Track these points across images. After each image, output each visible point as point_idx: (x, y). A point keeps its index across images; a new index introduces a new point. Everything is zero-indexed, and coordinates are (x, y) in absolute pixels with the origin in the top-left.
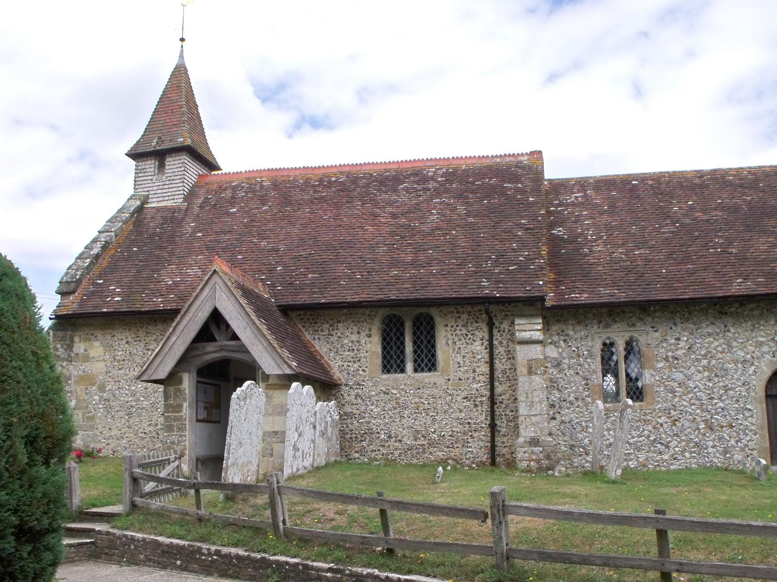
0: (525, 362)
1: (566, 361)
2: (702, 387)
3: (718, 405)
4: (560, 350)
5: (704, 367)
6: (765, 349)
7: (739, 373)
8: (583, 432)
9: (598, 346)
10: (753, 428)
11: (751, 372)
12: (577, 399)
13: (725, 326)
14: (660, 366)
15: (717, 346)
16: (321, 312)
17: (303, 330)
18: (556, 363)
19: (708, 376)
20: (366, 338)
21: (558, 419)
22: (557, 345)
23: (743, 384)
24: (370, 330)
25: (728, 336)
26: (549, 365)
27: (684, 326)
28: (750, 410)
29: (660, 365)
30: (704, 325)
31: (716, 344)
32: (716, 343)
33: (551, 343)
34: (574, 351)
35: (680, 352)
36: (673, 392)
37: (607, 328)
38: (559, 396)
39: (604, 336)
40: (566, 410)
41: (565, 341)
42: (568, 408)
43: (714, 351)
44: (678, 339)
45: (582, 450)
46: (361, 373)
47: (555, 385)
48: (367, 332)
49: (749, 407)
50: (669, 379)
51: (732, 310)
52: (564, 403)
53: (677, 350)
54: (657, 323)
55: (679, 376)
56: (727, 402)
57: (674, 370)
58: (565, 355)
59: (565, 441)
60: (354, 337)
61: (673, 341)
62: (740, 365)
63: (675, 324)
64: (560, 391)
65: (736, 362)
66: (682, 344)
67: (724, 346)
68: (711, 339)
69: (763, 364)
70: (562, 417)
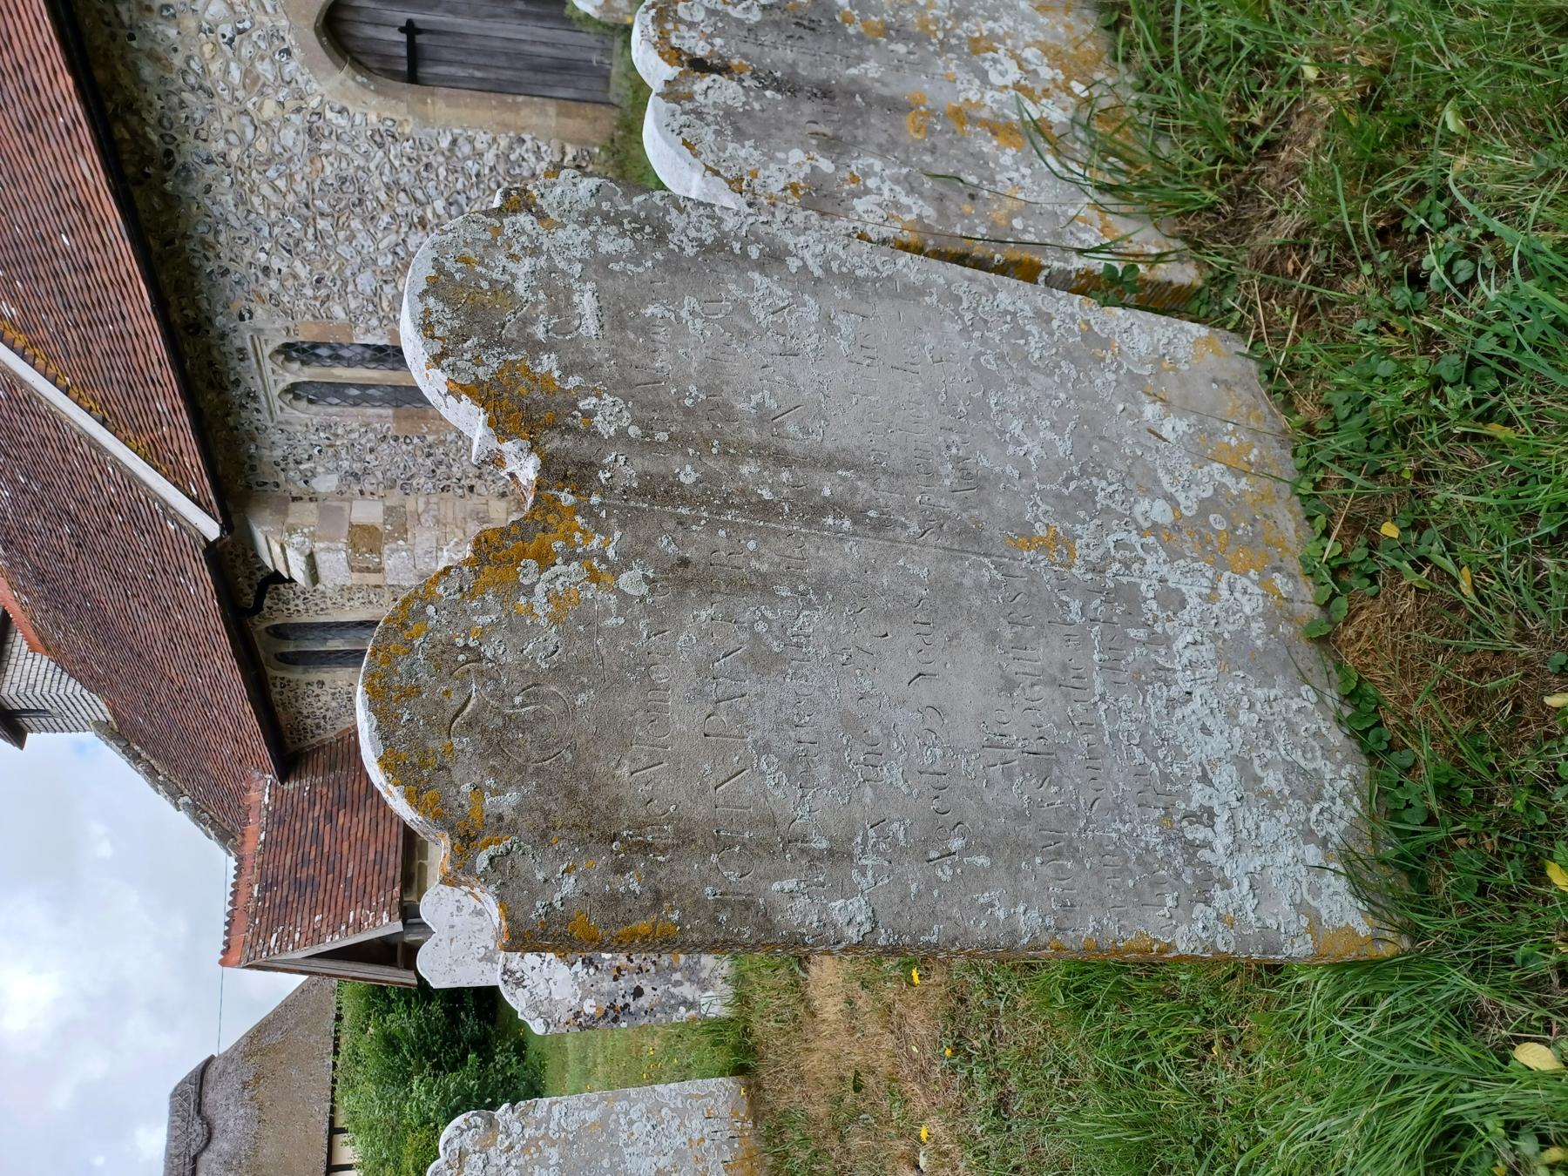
0: (355, 575)
1: (345, 464)
2: (393, 238)
3: (441, 211)
4: (320, 469)
5: (335, 226)
6: (265, 69)
7: (348, 150)
9: (302, 415)
10: (503, 143)
11: (342, 121)
12: (429, 455)
13: (209, 161)
14: (342, 315)
15: (275, 189)
16: (283, 719)
17: (318, 738)
18: (351, 478)
19: (363, 222)
20: (326, 687)
21: (473, 483)
22: (309, 474)
23: (381, 146)
25: (240, 159)
26: (356, 488)
27: (225, 253)
28: (454, 142)
29: (338, 311)
30: (216, 210)
31: (267, 189)
32: (266, 190)
33: (306, 482)
34: (320, 451)
35: (302, 271)
37: (255, 398)
38: (422, 481)
39: (278, 403)
40: (454, 469)
41: (298, 463)
42: (450, 466)
43: (291, 198)
44: (266, 270)
47: (400, 482)
48: (315, 687)
49: (445, 143)
50: (376, 300)
51: (155, 138)
52: (438, 472)
53: (295, 277)
54: (226, 306)
55: (366, 281)
56: (433, 192)
57: (351, 288)
58: (331, 465)
60: (323, 699)
61: (274, 284)
62: (325, 146)
63: (225, 272)
64: (412, 476)
65: (315, 154)
66: (276, 263)
67: (271, 173)
68: (256, 201)
69: (315, 86)
70: (467, 477)
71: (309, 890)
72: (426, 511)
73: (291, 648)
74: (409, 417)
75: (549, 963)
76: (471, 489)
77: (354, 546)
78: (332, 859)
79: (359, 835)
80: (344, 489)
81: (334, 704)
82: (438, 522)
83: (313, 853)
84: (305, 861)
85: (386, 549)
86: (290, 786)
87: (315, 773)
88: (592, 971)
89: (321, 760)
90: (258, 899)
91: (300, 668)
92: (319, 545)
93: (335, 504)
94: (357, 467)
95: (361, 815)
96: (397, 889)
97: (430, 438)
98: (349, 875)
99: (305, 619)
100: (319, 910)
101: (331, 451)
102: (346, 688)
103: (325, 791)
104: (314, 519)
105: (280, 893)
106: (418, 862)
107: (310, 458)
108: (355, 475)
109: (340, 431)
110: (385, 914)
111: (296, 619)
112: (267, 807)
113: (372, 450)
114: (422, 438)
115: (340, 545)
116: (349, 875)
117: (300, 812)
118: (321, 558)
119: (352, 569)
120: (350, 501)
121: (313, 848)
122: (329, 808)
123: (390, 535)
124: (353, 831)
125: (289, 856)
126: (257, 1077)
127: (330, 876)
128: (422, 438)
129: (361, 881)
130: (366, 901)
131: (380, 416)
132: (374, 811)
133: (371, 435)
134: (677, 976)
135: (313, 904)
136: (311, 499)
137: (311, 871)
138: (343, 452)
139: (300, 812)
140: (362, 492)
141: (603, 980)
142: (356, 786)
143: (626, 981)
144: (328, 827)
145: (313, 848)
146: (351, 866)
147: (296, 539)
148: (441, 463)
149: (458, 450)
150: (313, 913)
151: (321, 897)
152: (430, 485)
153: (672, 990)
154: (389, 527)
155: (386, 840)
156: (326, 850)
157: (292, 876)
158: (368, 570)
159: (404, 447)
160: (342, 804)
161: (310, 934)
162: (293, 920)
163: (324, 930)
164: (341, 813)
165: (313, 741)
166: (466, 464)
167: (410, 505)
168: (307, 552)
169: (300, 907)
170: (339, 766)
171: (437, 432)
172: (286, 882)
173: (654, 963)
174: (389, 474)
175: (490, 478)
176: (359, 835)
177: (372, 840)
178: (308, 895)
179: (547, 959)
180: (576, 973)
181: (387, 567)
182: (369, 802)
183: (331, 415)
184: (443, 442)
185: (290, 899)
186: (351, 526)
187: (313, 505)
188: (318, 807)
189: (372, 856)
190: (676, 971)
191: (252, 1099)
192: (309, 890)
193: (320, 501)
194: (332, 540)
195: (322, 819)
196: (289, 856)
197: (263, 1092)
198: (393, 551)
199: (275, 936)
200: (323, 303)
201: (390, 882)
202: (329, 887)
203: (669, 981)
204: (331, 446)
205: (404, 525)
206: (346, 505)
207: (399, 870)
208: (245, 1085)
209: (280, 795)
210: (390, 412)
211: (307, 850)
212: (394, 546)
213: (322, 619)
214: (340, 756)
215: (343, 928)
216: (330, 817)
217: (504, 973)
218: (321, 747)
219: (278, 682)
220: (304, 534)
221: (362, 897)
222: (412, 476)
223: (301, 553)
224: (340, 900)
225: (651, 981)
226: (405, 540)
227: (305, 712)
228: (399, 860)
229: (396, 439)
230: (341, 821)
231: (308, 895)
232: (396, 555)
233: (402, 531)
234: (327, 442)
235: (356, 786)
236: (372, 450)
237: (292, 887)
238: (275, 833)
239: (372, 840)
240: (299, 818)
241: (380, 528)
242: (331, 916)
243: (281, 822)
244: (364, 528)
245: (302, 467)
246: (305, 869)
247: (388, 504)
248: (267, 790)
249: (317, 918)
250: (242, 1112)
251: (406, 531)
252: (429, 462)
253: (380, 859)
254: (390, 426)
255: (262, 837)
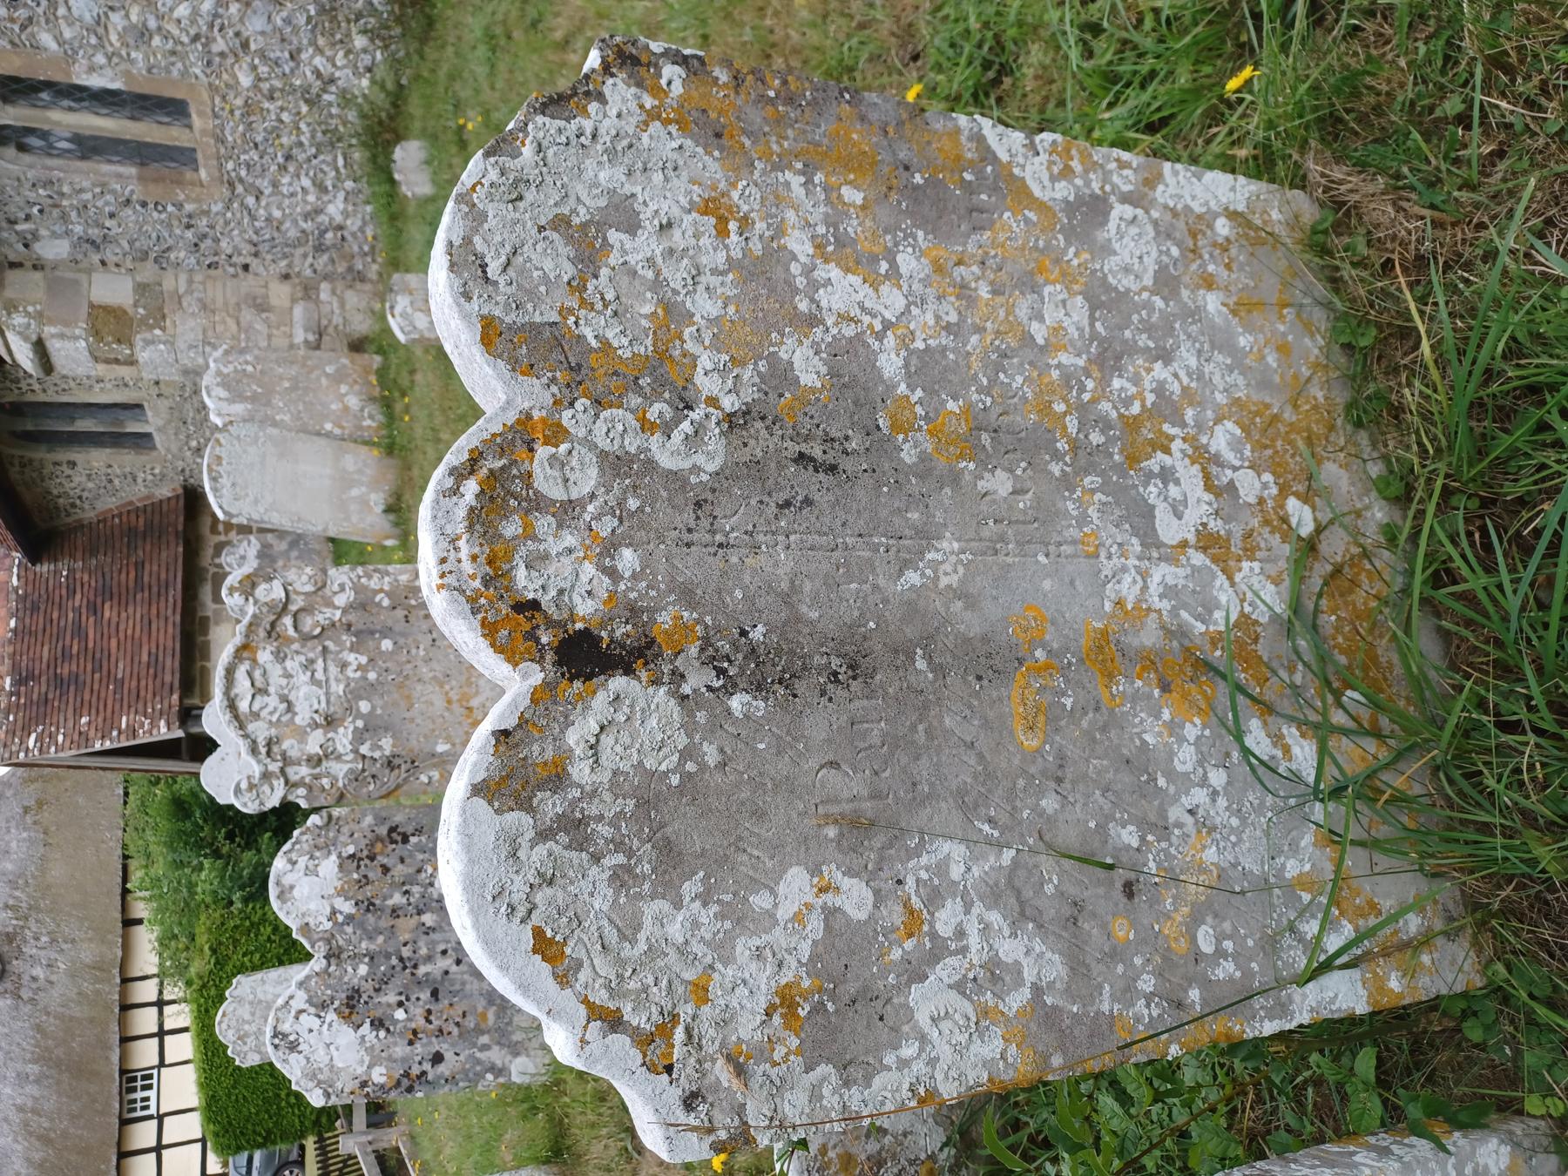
1: (78, 229)
4: (43, 232)
8: (283, 228)
12: (189, 226)
14: (53, 46)
20: (79, 468)
22: (29, 237)
24: (56, 464)
26: (96, 258)
29: (46, 39)
33: (26, 246)
34: (41, 211)
36: (143, 35)
38: (182, 254)
40: (224, 244)
45: (329, 235)
46: (157, 471)
50: (101, 30)
52: (203, 246)
57: (61, 11)
59: (305, 256)
60: (77, 479)
64: (169, 249)
70: (240, 254)
71: (72, 688)
72: (189, 291)
73: (30, 427)
74: (157, 180)
75: (330, 1025)
76: (246, 267)
77: (96, 333)
78: (98, 655)
79: (129, 632)
80: (80, 257)
81: (90, 485)
82: (204, 307)
83: (75, 648)
84: (66, 655)
85: (138, 340)
86: (44, 568)
87: (72, 557)
88: (382, 1034)
89: (79, 542)
90: (12, 694)
91: (44, 447)
92: (49, 330)
93: (69, 275)
94: (94, 233)
95: (131, 610)
96: (175, 697)
97: (189, 207)
98: (120, 676)
99: (42, 398)
100: (85, 711)
101: (56, 212)
102: (104, 470)
103: (86, 578)
104: (40, 294)
105: (38, 689)
106: (199, 664)
107: (28, 218)
108: (93, 243)
109: (66, 189)
110: (162, 723)
111: (30, 398)
112: (16, 590)
113: (112, 216)
114: (179, 206)
115: (77, 332)
116: (120, 676)
117: (57, 600)
118: (54, 346)
119: (96, 359)
120: (89, 271)
121: (76, 642)
122: (92, 598)
123: (143, 321)
124: (122, 627)
125: (46, 649)
126: (40, 804)
127: (97, 676)
128: (179, 206)
129: (134, 683)
130: (140, 707)
131: (119, 176)
132: (146, 606)
133: (109, 197)
134: (484, 1039)
135: (78, 704)
136: (35, 267)
137: (74, 667)
138: (74, 214)
139: (57, 600)
140: (103, 263)
141: (395, 1044)
142: (123, 576)
143: (423, 1046)
144: (92, 619)
145: (76, 642)
146: (121, 665)
147: (18, 320)
148: (205, 236)
149: (227, 223)
150: (78, 714)
151: (87, 697)
152: (193, 260)
153: (478, 1055)
154: (141, 311)
155: (161, 641)
156: (91, 645)
157: (52, 671)
158: (117, 361)
159: (155, 214)
160: (107, 595)
161: (76, 737)
162: (55, 720)
163: (92, 733)
164: (107, 605)
165: (70, 520)
166: (237, 239)
167: (168, 283)
168: (34, 338)
169: (63, 707)
170: (102, 550)
171: (198, 200)
172: (44, 679)
173: (457, 1024)
174: (137, 244)
175: (269, 257)
176: (129, 632)
177: (145, 639)
178: (71, 695)
179: (328, 1020)
180: (363, 1037)
181: (141, 360)
182: (139, 596)
183: (51, 169)
184: (207, 213)
185: (50, 696)
186: (92, 306)
187: (38, 275)
188: (78, 596)
189: (145, 658)
190: (483, 1033)
191: (35, 823)
192: (72, 688)
193: (48, 270)
194: (66, 324)
195: (84, 610)
196: (46, 649)
197: (46, 816)
198: (148, 343)
199: (33, 736)
200: (23, 27)
201: (167, 688)
202: (96, 687)
203: (474, 1045)
204: (56, 206)
205: (161, 309)
206: (83, 277)
207: (177, 676)
208: (26, 810)
209: (31, 577)
210: (132, 171)
211: (68, 642)
212: (148, 336)
213: (65, 399)
214: (103, 540)
215: (115, 733)
216: (94, 609)
217: (275, 1036)
218: (80, 526)
219: (16, 462)
220: (28, 314)
221: (136, 701)
222: (169, 249)
223: (26, 339)
224: (110, 703)
225: (453, 1045)
226: (163, 329)
227: (55, 492)
228: (177, 664)
229: (144, 204)
230: (107, 614)
231: (71, 695)
232: (152, 347)
233: (158, 317)
234: (50, 201)
235: (123, 576)
236: (112, 216)
237: (52, 683)
238: (27, 621)
239: (145, 639)
240: (56, 607)
241: (130, 311)
242: (100, 720)
243: (35, 608)
244: (108, 310)
245: (19, 227)
246: (66, 665)
247: (138, 279)
248: (15, 570)
249: (84, 720)
250: (25, 835)
251: (164, 317)
252: (189, 234)
253: (155, 663)
254: (134, 189)
255: (13, 623)
